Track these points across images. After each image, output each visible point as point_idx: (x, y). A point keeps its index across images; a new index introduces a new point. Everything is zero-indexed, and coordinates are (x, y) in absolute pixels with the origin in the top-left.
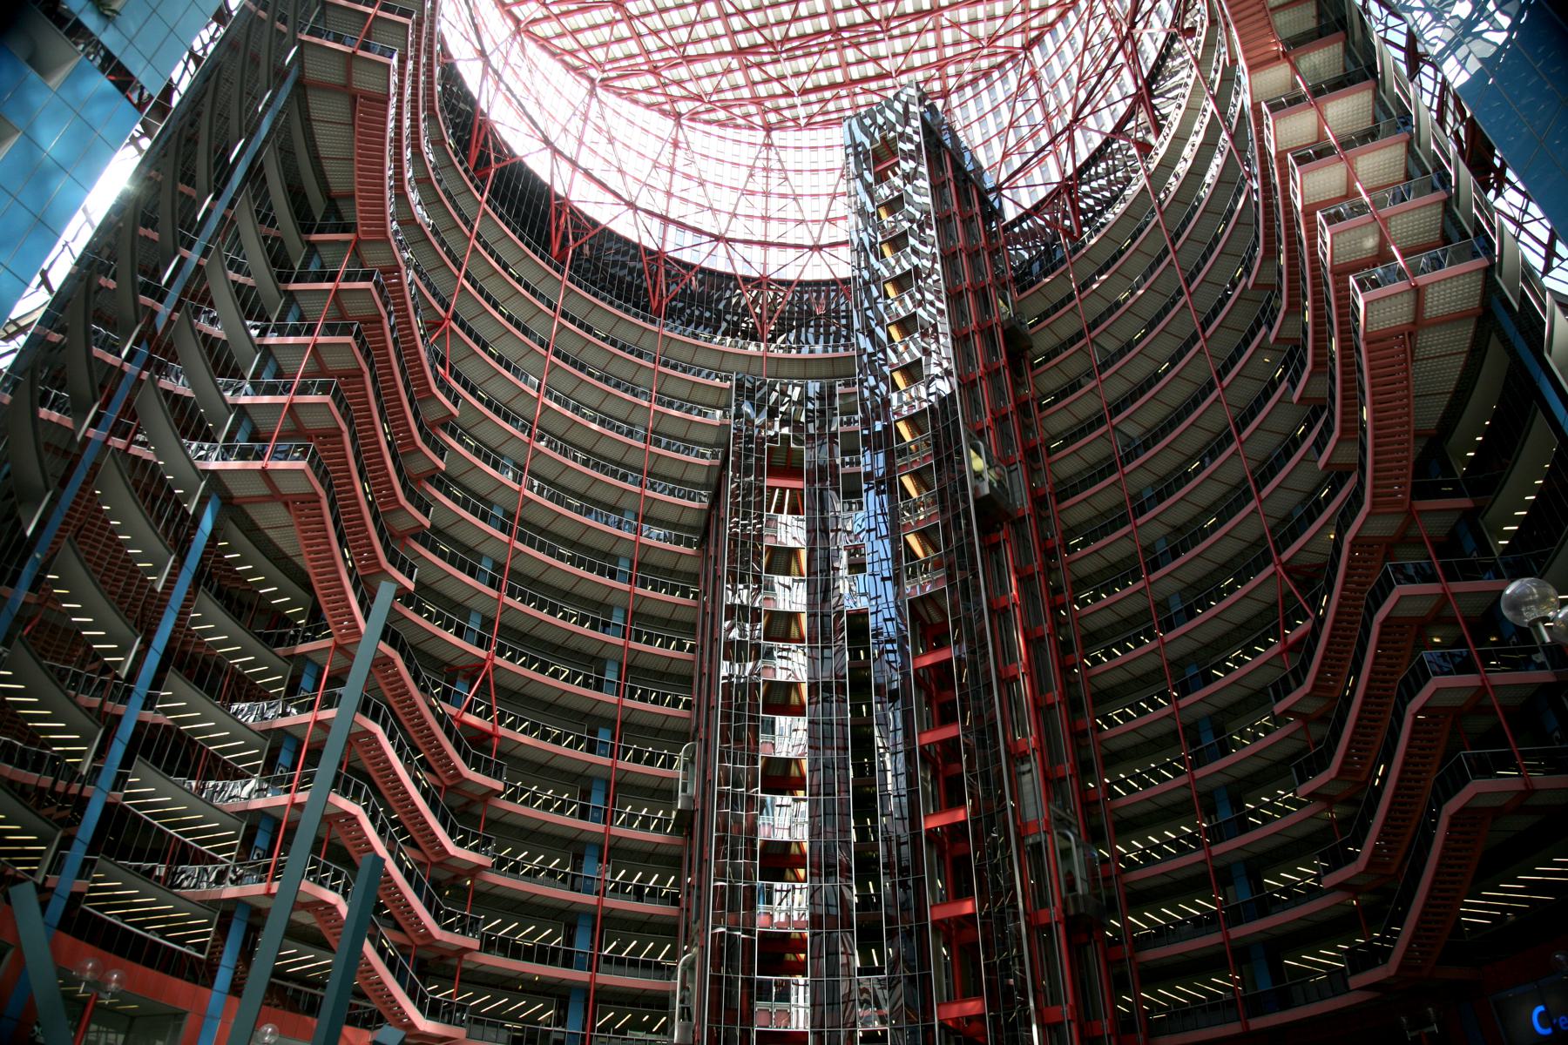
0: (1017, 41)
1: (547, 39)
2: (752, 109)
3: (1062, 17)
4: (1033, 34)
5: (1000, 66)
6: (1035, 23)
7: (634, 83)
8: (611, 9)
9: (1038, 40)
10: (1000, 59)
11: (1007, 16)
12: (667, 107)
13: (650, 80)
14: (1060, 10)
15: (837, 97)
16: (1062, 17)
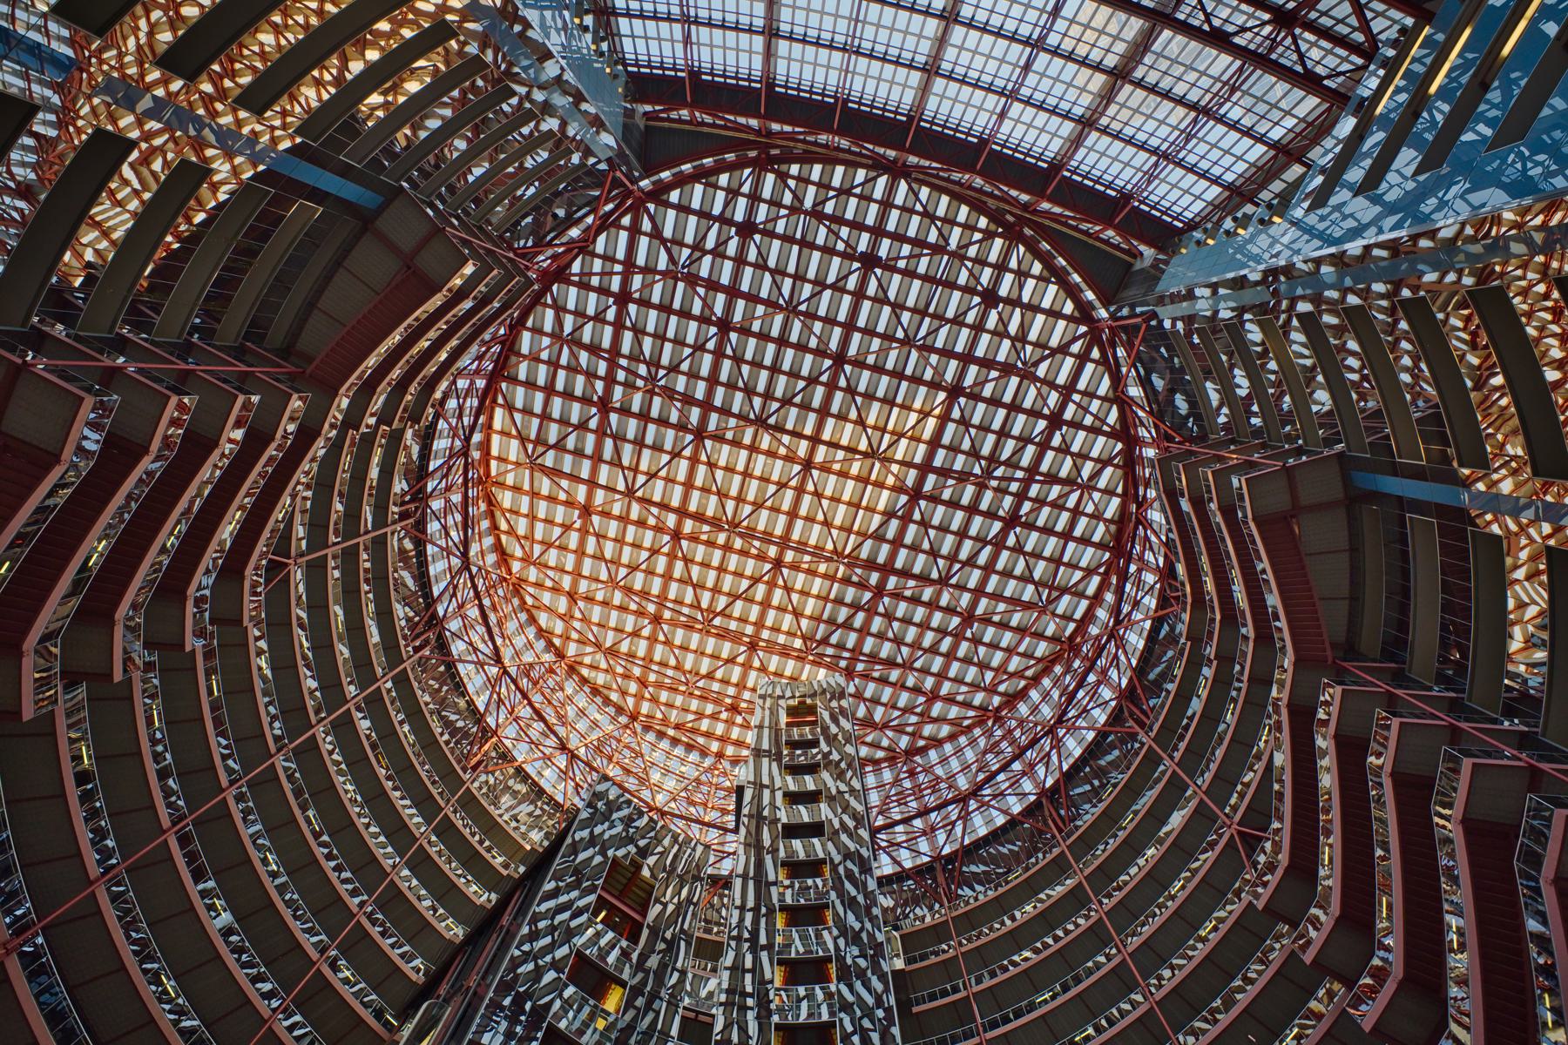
0: (904, 742)
1: (503, 512)
2: (633, 687)
3: (952, 737)
4: (921, 743)
5: (876, 762)
6: (928, 730)
7: (546, 598)
8: (577, 512)
9: (923, 751)
10: (880, 754)
11: (905, 711)
12: (557, 642)
13: (562, 605)
14: (954, 729)
15: (714, 717)
16: (952, 737)
